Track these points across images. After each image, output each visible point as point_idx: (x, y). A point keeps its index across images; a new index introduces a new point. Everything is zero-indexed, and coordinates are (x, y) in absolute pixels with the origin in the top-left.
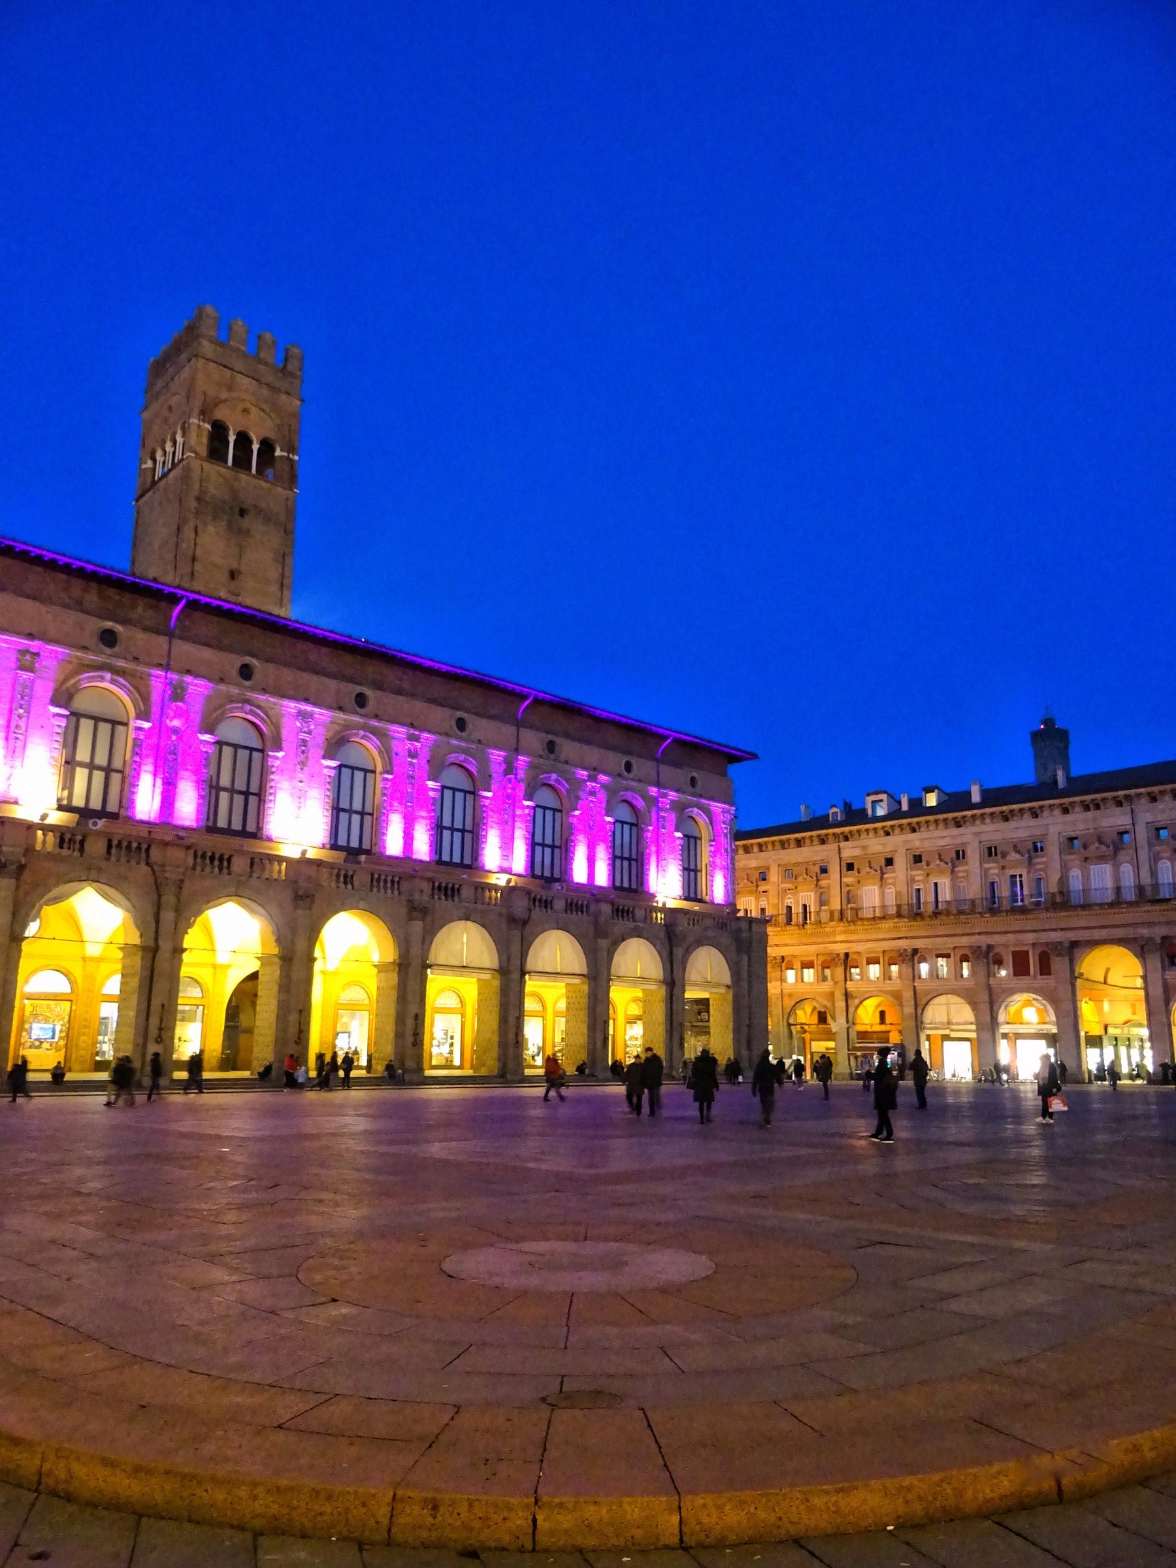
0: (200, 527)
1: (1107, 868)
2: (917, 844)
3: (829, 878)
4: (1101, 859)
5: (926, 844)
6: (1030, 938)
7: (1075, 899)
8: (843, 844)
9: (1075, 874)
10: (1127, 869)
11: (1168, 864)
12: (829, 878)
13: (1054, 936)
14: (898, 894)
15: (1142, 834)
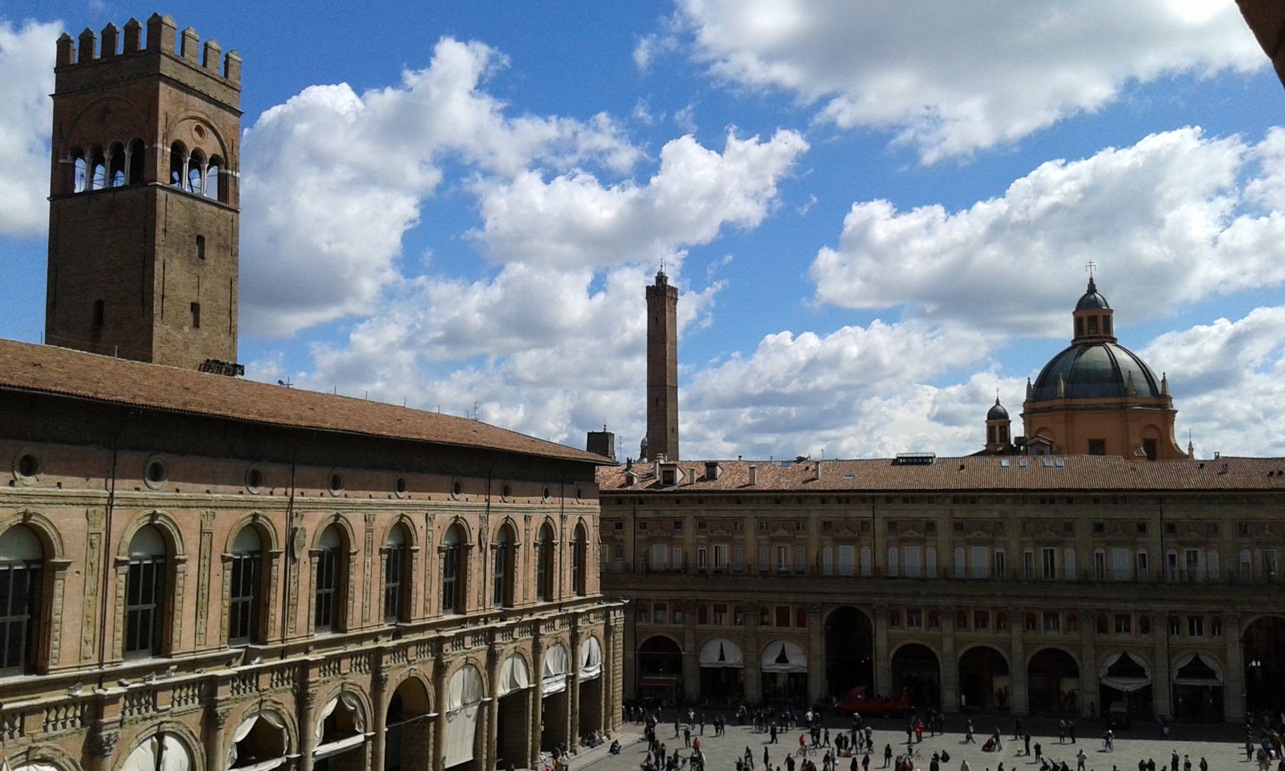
0: (168, 261)
1: (851, 549)
2: (703, 513)
3: (623, 533)
4: (849, 541)
5: (711, 514)
6: (791, 598)
7: (828, 571)
8: (638, 506)
9: (828, 552)
10: (866, 552)
11: (896, 549)
12: (623, 533)
13: (810, 598)
14: (686, 555)
15: (880, 526)
